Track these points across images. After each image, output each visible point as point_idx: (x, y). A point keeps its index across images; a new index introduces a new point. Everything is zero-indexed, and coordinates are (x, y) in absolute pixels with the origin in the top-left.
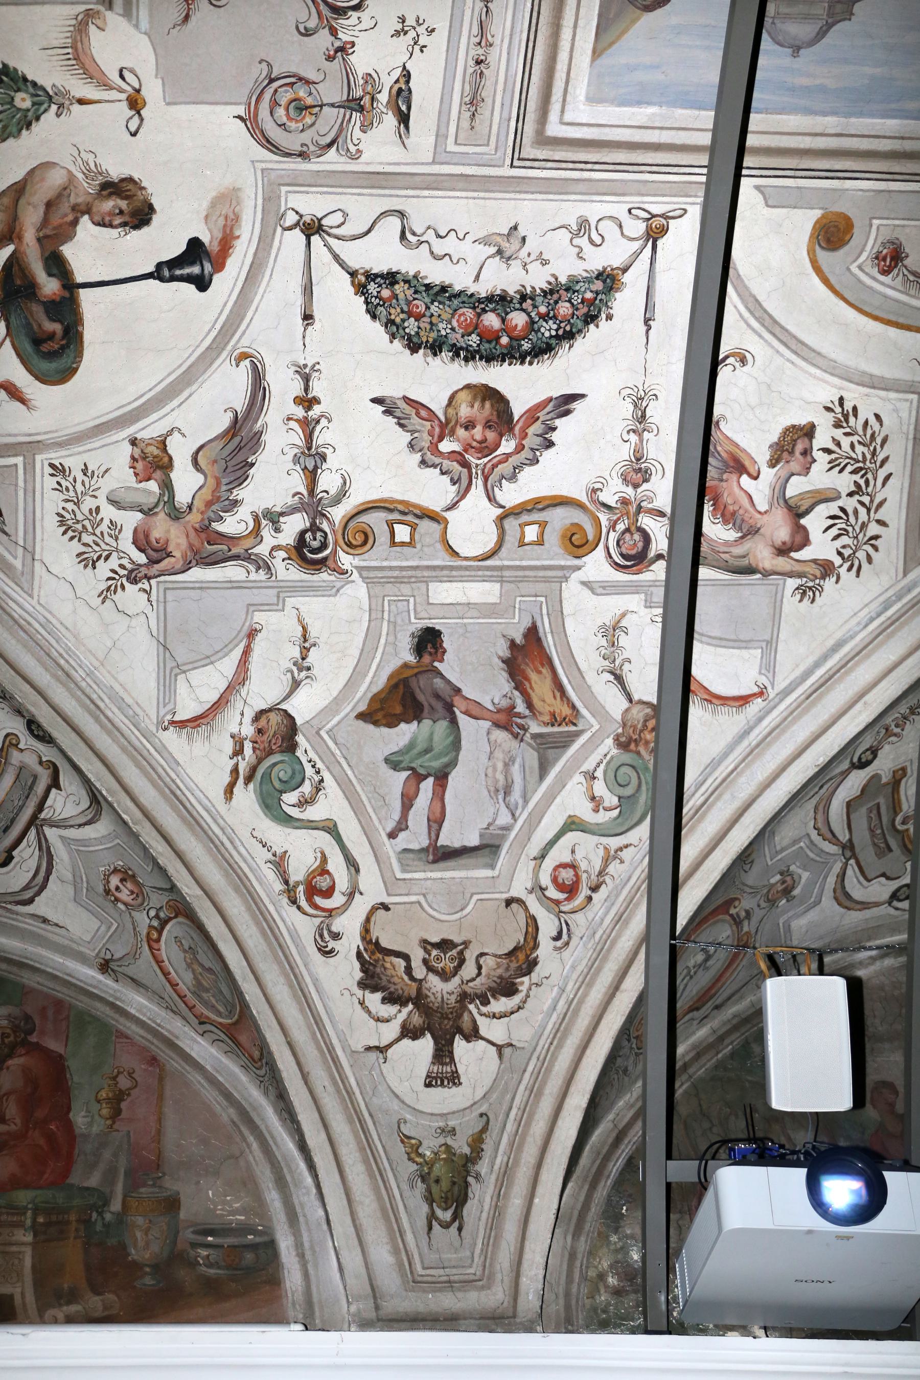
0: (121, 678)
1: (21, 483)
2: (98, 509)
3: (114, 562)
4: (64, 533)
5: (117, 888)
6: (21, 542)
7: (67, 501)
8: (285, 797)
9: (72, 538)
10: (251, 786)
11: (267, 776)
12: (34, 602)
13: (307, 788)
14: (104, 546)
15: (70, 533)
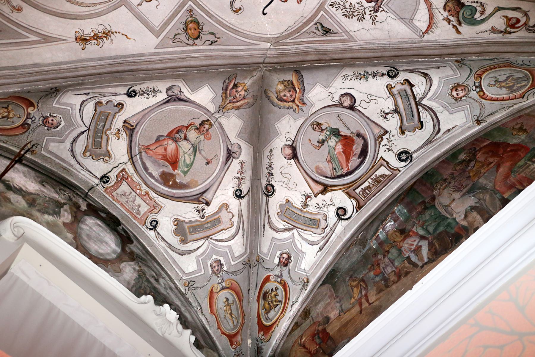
0: (399, 37)
1: (327, 17)
2: (351, 3)
3: (368, 12)
4: (349, 18)
5: (457, 94)
6: (341, 31)
7: (342, 10)
8: (475, 17)
9: (352, 18)
10: (463, 25)
11: (464, 18)
12: (359, 42)
13: (479, 9)
14: (361, 11)
15: (350, 17)
